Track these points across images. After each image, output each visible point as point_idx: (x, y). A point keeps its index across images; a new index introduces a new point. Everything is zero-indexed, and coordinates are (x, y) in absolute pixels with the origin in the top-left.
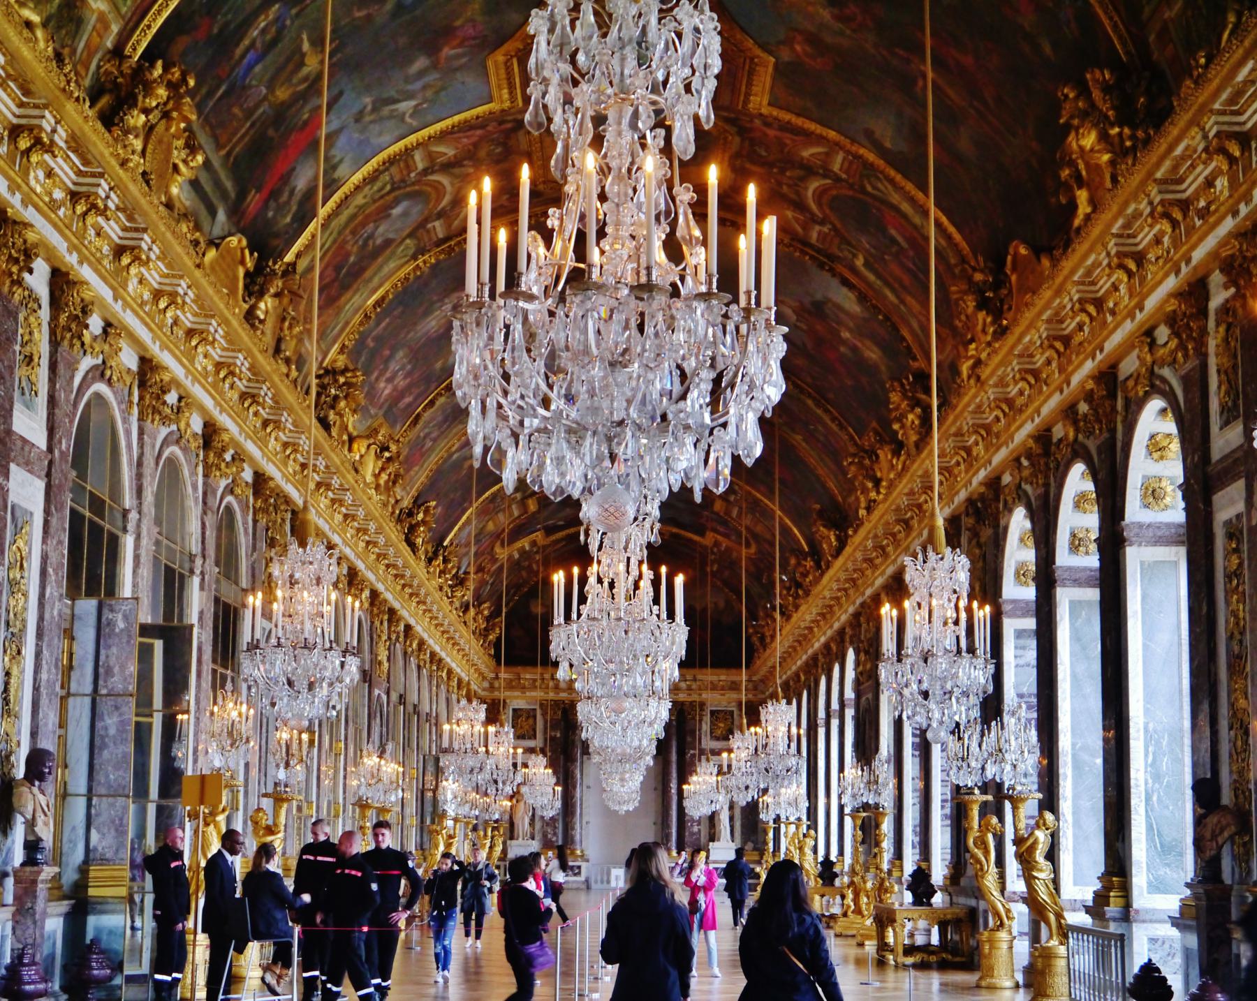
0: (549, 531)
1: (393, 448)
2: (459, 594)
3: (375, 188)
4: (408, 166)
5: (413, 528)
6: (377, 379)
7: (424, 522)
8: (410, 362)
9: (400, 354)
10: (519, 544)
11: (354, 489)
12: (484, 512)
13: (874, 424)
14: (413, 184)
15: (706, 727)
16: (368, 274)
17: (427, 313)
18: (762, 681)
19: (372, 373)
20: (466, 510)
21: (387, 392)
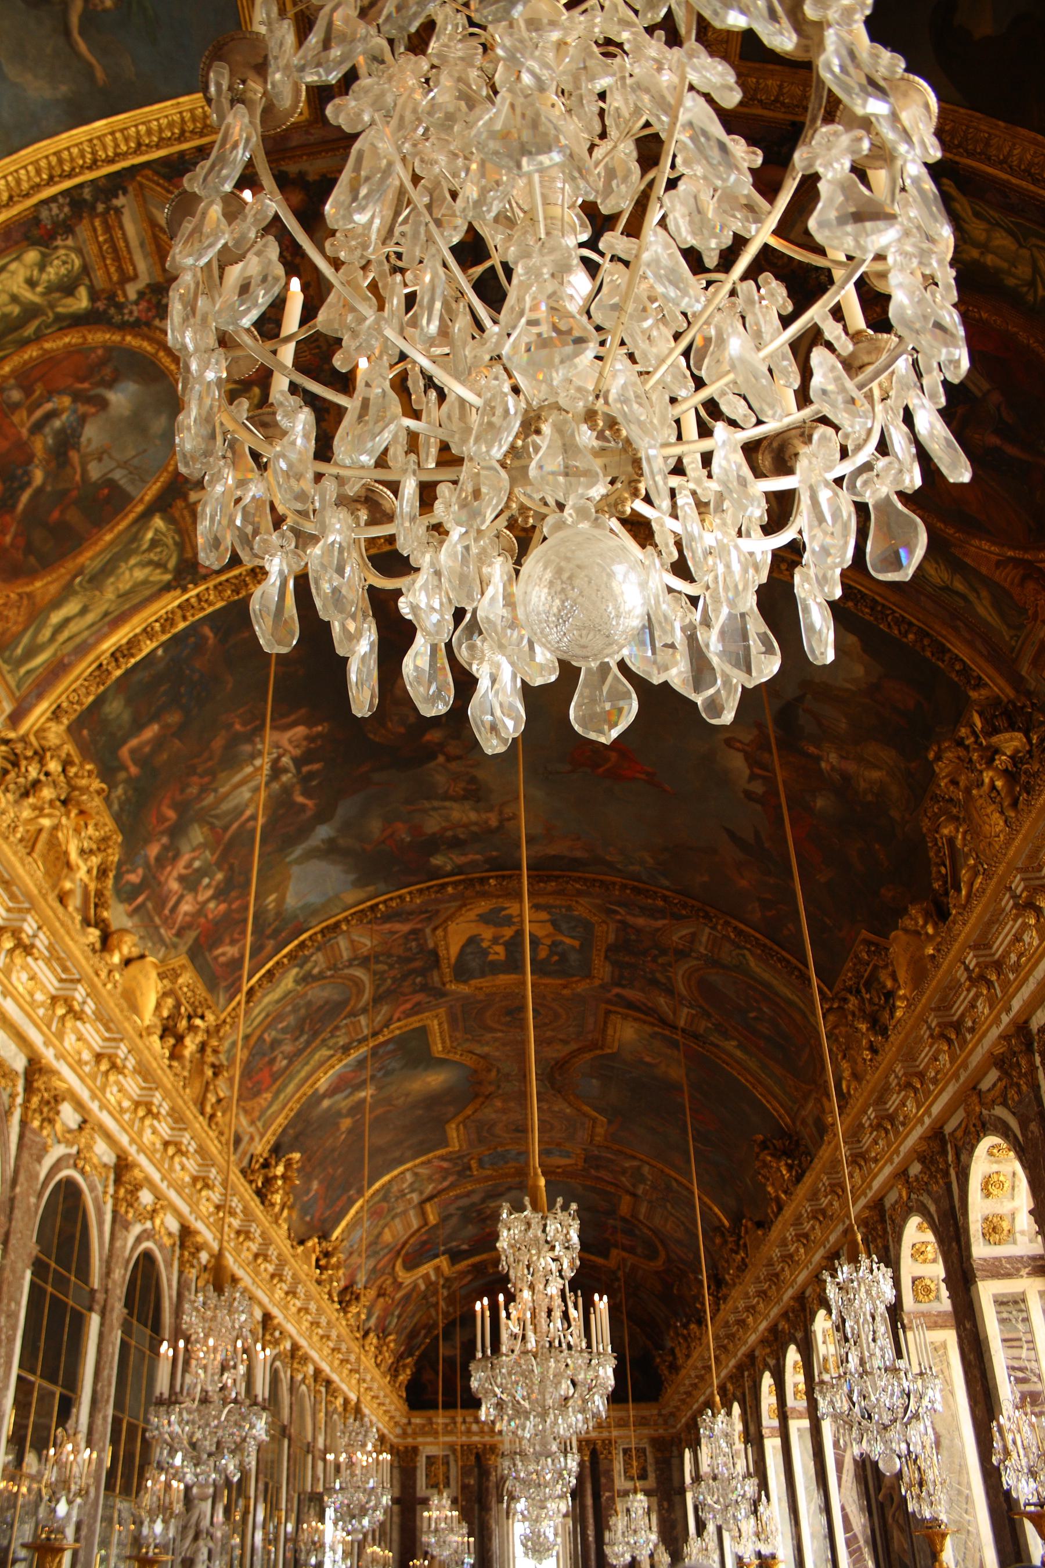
0: (455, 1257)
1: (210, 1017)
2: (354, 1309)
3: (53, 272)
4: (115, 249)
5: (268, 1181)
6: (161, 861)
7: (284, 1177)
8: (220, 868)
9: (197, 835)
10: (423, 1270)
11: (92, 985)
12: (377, 1212)
13: (865, 934)
14: (135, 327)
15: (618, 1466)
16: (89, 558)
17: (231, 761)
18: (672, 1414)
19: (147, 841)
20: (351, 1203)
21: (186, 907)
